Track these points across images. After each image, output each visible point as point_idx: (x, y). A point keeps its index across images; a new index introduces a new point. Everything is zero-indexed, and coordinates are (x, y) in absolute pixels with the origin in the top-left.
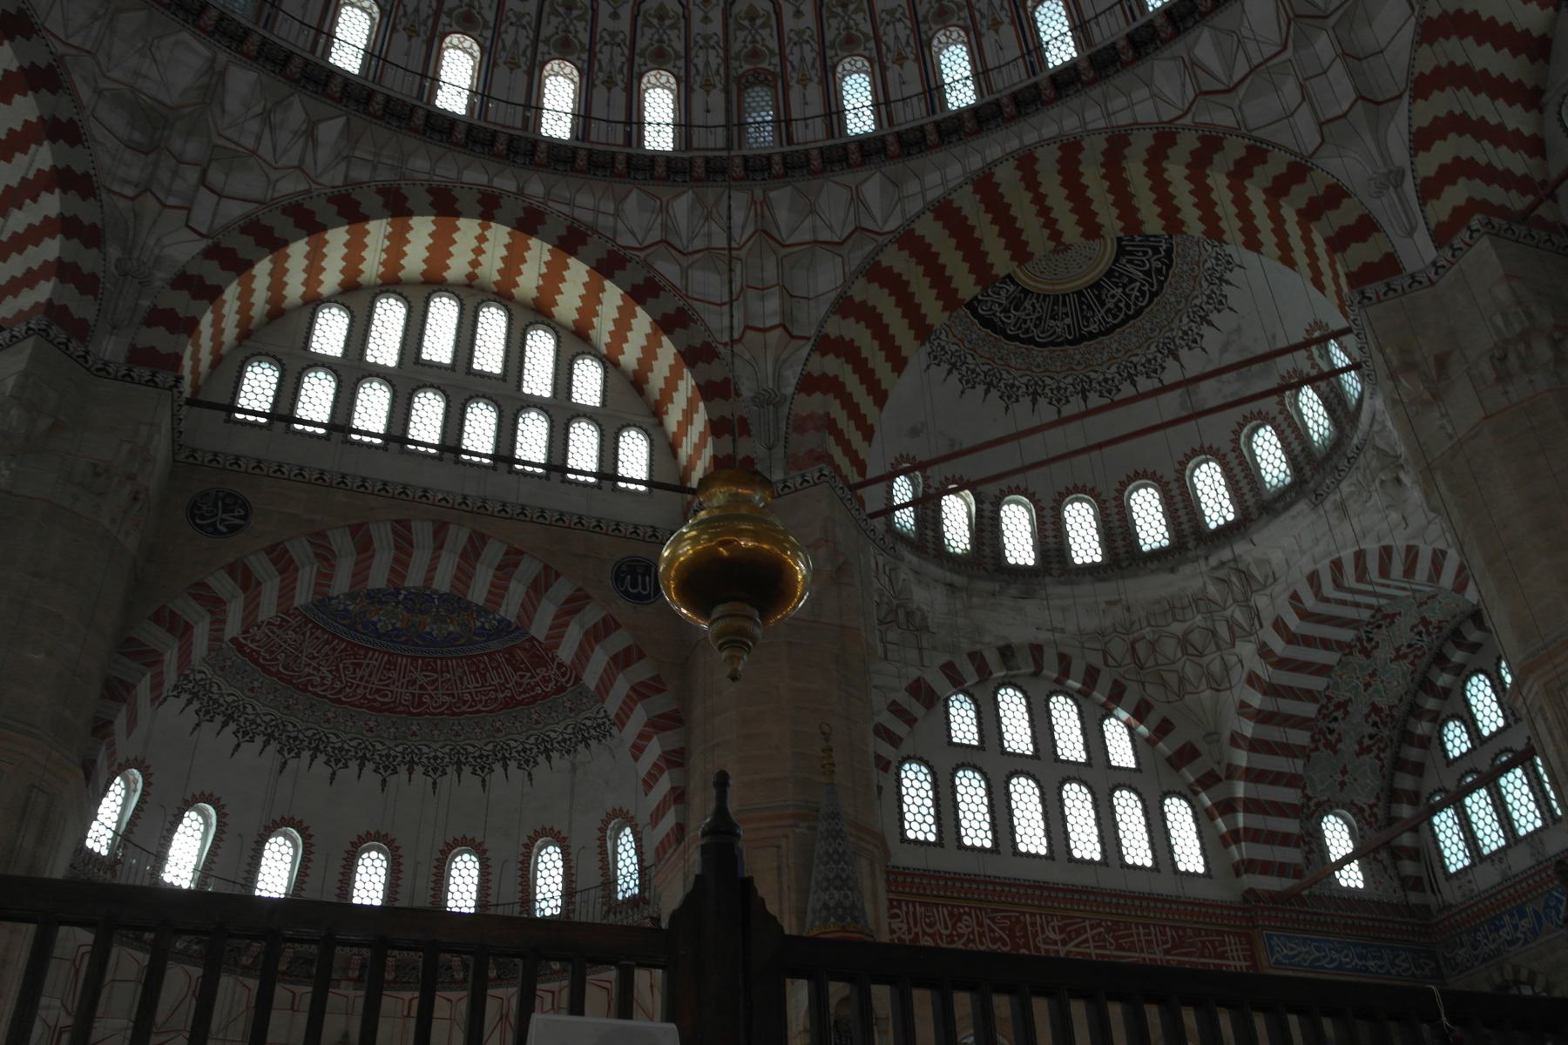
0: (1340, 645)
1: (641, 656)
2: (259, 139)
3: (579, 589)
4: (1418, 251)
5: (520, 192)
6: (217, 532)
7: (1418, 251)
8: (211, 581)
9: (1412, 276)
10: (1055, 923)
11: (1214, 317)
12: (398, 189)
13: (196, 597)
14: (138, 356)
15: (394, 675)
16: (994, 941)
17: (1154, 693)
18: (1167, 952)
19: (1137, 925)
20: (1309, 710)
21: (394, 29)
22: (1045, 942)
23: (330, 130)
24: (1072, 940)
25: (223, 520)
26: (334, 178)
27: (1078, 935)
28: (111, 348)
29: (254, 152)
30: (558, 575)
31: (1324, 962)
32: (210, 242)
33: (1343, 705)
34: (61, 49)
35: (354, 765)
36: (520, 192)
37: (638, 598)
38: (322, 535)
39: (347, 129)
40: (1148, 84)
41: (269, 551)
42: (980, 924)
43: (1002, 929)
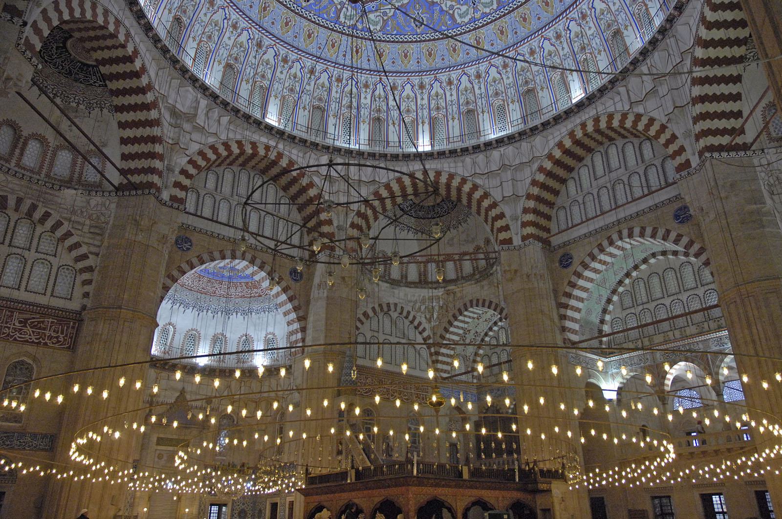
0: (474, 318)
2: (205, 123)
4: (517, 241)
5: (276, 147)
7: (517, 241)
8: (182, 265)
9: (514, 247)
11: (462, 224)
12: (241, 141)
14: (173, 198)
15: (209, 284)
20: (461, 332)
21: (242, 80)
23: (225, 120)
26: (223, 137)
28: (165, 196)
29: (204, 128)
32: (189, 158)
33: (469, 331)
34: (157, 95)
35: (191, 308)
36: (276, 147)
37: (295, 280)
38: (212, 253)
39: (230, 122)
40: (463, 162)
41: (198, 257)
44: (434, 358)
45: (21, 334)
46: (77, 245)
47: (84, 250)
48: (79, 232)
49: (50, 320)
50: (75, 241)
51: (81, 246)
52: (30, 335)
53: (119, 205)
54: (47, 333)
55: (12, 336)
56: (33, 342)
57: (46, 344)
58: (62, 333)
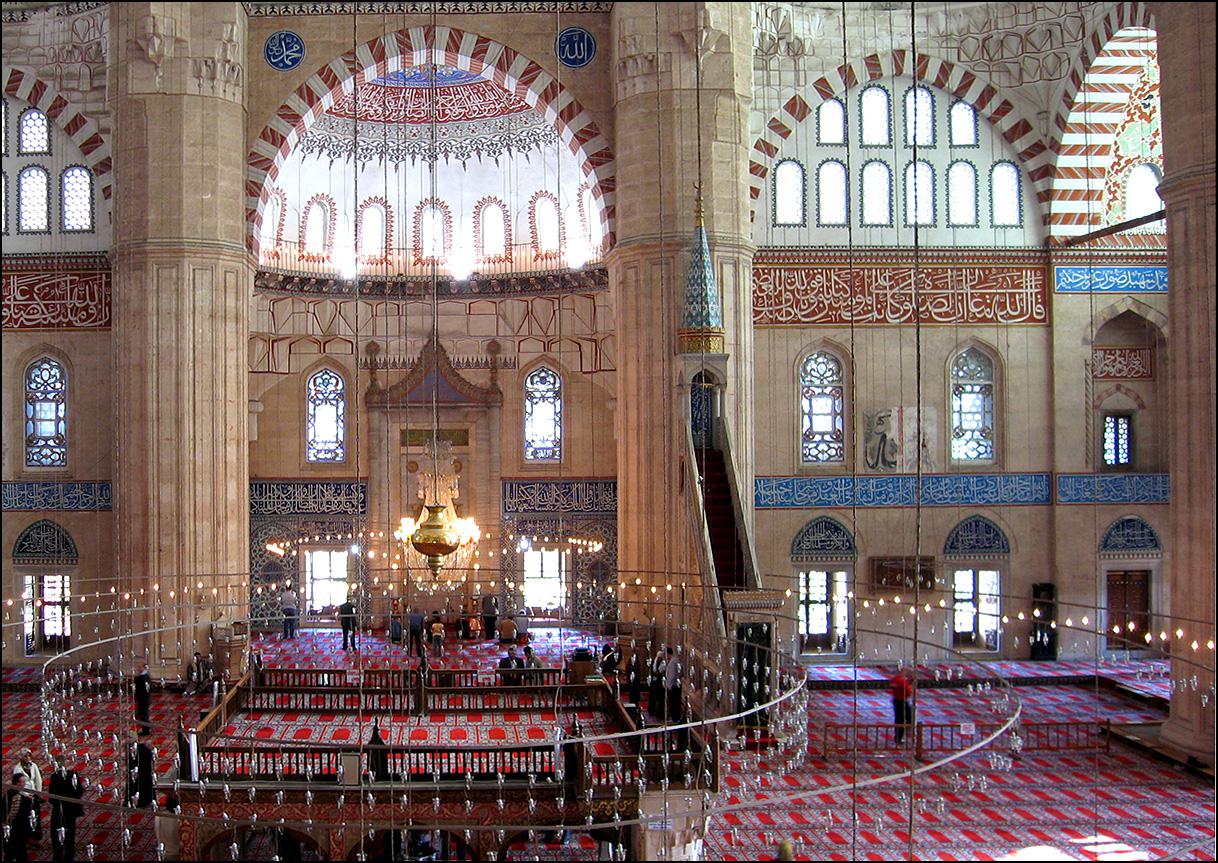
1: (581, 109)
3: (532, 62)
6: (286, 66)
8: (290, 103)
10: (887, 274)
13: (283, 116)
16: (837, 291)
17: (998, 80)
18: (972, 287)
19: (952, 270)
22: (877, 288)
24: (898, 285)
25: (287, 56)
27: (904, 279)
30: (515, 54)
31: (1101, 286)
42: (829, 280)
43: (846, 282)
44: (1040, 186)
45: (28, 314)
46: (76, 124)
47: (89, 130)
48: (76, 96)
49: (69, 278)
50: (71, 116)
51: (85, 122)
52: (43, 313)
53: (115, 21)
54: (69, 303)
55: (16, 321)
56: (50, 325)
57: (70, 324)
58: (92, 298)
